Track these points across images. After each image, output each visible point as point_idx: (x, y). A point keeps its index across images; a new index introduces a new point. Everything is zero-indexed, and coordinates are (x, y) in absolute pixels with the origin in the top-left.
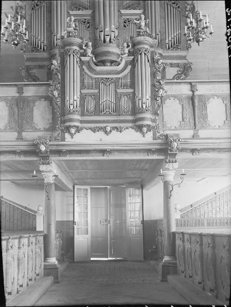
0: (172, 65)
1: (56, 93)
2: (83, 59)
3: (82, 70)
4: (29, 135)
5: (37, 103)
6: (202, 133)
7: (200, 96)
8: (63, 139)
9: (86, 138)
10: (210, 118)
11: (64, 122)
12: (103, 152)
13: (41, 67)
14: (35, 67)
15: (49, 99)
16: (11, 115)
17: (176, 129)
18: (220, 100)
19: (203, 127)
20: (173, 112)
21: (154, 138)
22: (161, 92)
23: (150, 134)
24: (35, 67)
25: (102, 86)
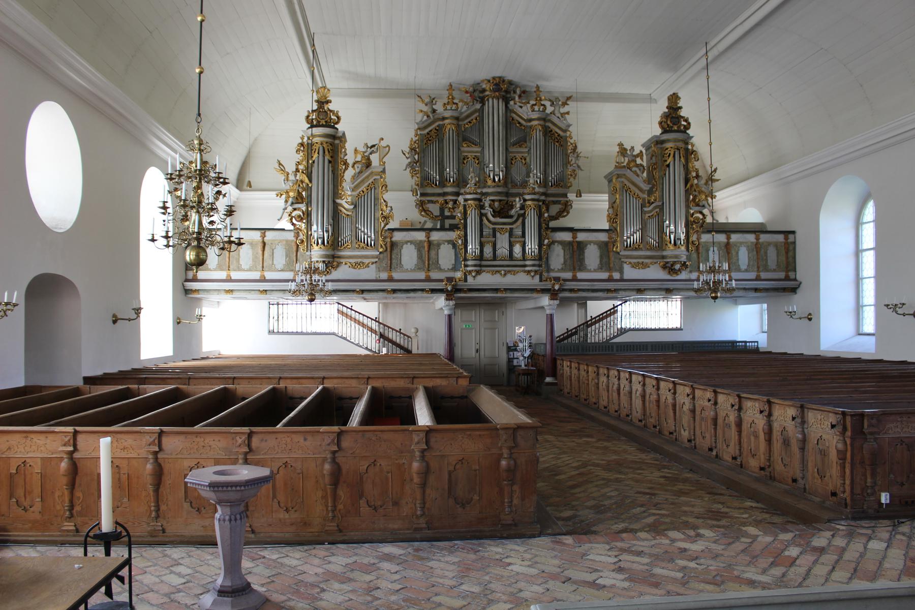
0: (555, 203)
1: (460, 242)
2: (483, 211)
3: (481, 220)
4: (434, 275)
5: (442, 246)
6: (580, 275)
7: (579, 243)
8: (466, 280)
9: (486, 279)
10: (587, 262)
11: (466, 266)
12: (496, 290)
13: (432, 202)
14: (430, 202)
15: (454, 246)
16: (420, 257)
17: (559, 271)
18: (596, 246)
19: (580, 270)
20: (557, 258)
21: (541, 281)
22: (546, 241)
23: (538, 277)
24: (430, 202)
25: (498, 234)
